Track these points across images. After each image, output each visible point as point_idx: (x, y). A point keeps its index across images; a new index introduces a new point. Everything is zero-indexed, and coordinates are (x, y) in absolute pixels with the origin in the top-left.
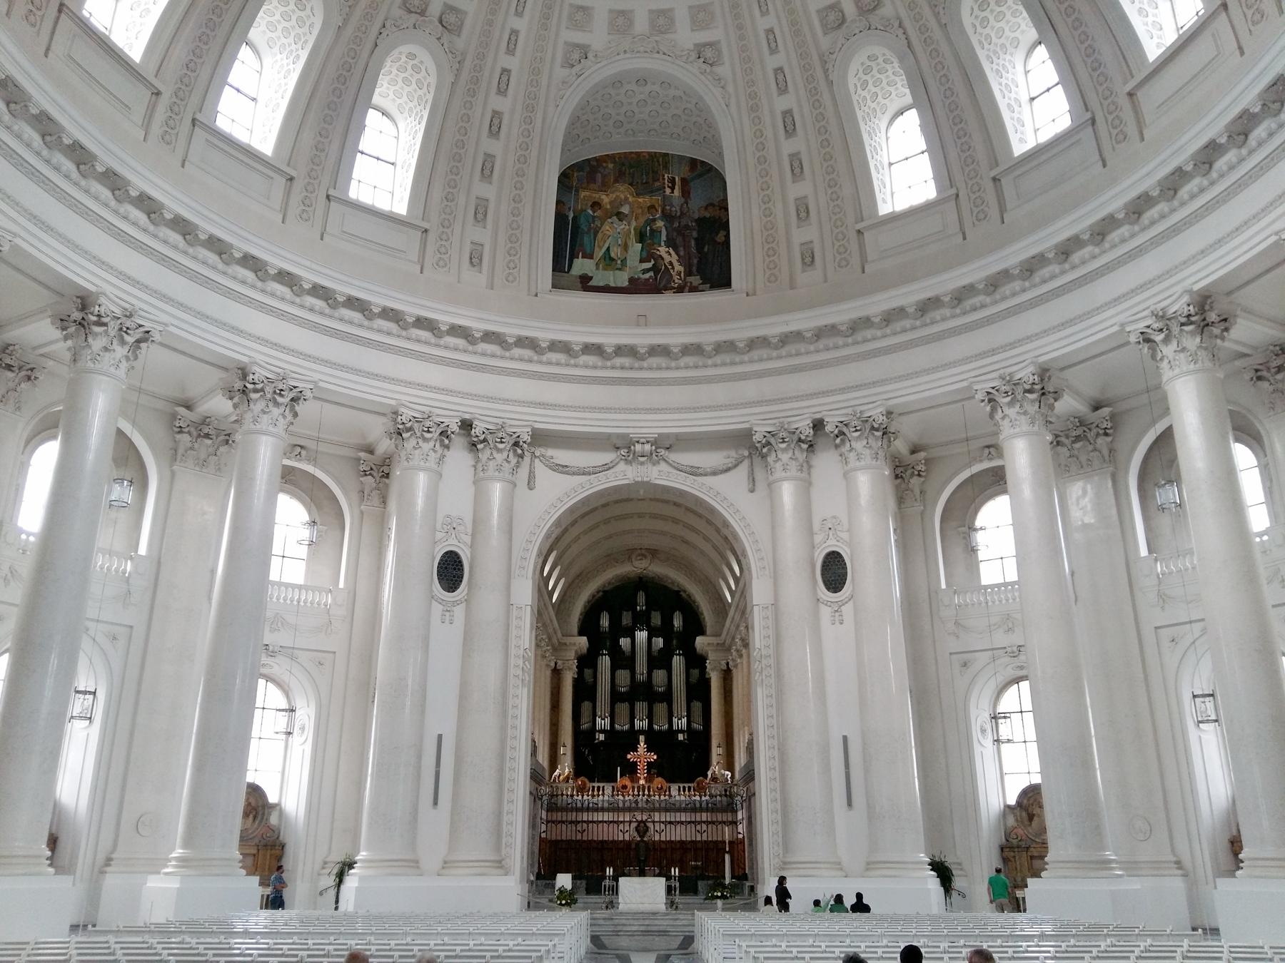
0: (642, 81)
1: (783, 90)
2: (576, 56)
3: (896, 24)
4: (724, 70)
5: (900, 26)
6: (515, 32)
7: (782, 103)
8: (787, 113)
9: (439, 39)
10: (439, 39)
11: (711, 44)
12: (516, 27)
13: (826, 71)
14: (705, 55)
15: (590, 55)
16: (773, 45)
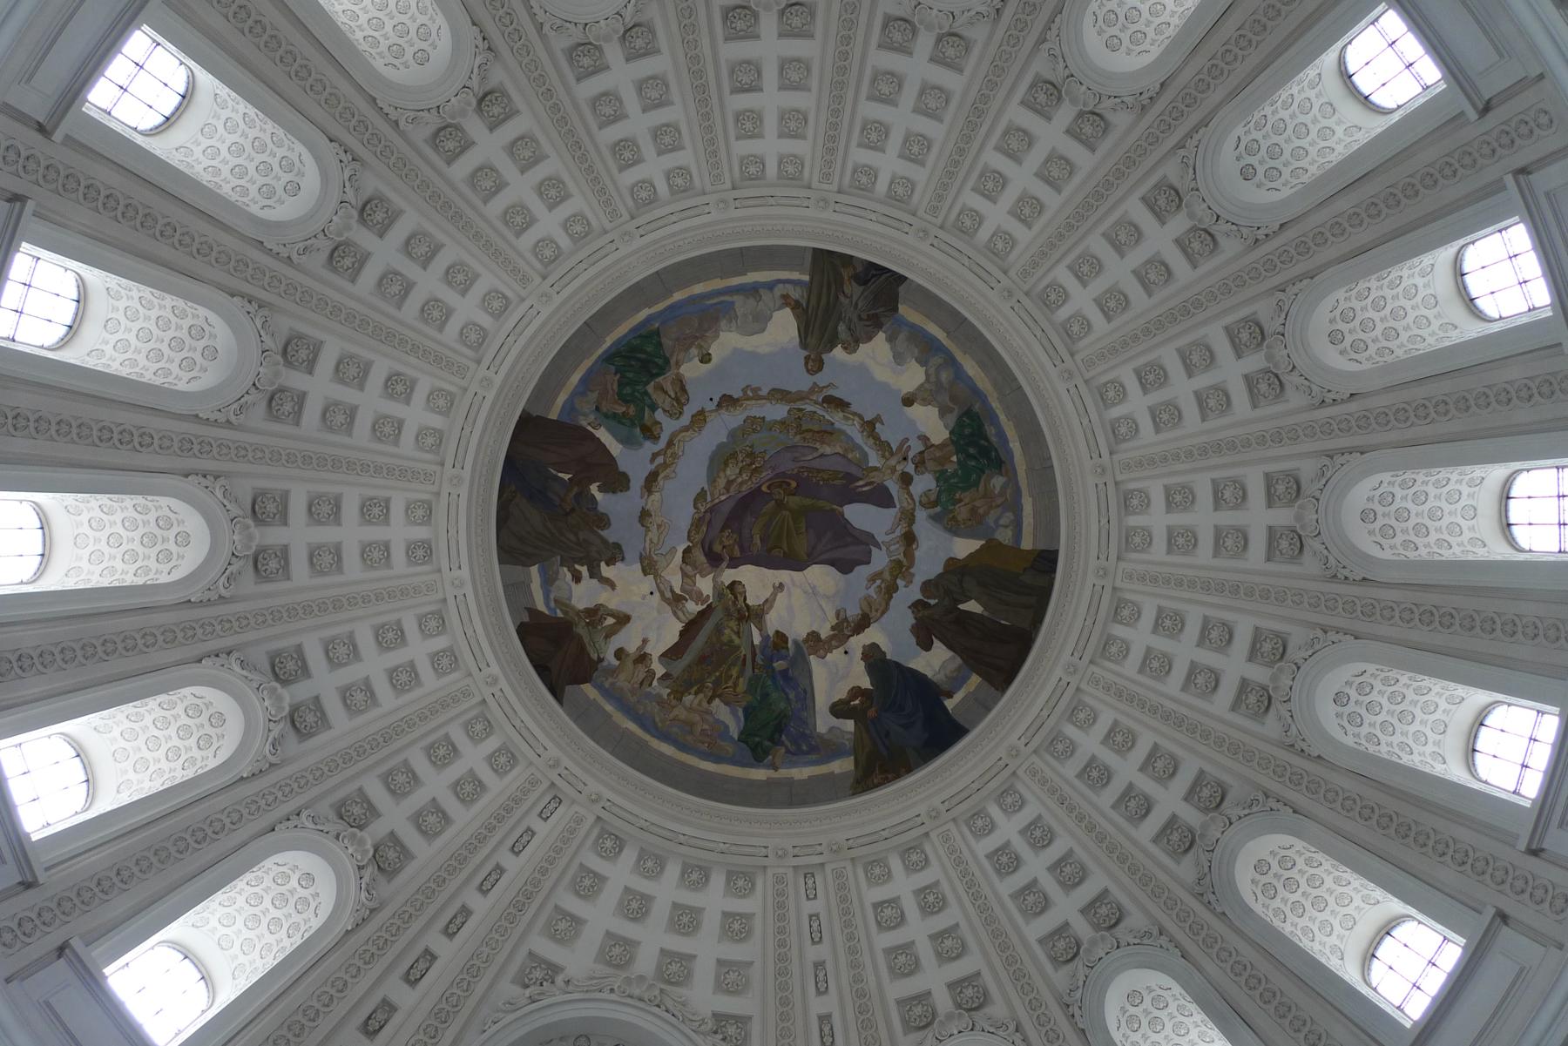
2: (538, 974)
6: (466, 912)
9: (360, 868)
10: (360, 868)
12: (471, 905)
15: (559, 979)
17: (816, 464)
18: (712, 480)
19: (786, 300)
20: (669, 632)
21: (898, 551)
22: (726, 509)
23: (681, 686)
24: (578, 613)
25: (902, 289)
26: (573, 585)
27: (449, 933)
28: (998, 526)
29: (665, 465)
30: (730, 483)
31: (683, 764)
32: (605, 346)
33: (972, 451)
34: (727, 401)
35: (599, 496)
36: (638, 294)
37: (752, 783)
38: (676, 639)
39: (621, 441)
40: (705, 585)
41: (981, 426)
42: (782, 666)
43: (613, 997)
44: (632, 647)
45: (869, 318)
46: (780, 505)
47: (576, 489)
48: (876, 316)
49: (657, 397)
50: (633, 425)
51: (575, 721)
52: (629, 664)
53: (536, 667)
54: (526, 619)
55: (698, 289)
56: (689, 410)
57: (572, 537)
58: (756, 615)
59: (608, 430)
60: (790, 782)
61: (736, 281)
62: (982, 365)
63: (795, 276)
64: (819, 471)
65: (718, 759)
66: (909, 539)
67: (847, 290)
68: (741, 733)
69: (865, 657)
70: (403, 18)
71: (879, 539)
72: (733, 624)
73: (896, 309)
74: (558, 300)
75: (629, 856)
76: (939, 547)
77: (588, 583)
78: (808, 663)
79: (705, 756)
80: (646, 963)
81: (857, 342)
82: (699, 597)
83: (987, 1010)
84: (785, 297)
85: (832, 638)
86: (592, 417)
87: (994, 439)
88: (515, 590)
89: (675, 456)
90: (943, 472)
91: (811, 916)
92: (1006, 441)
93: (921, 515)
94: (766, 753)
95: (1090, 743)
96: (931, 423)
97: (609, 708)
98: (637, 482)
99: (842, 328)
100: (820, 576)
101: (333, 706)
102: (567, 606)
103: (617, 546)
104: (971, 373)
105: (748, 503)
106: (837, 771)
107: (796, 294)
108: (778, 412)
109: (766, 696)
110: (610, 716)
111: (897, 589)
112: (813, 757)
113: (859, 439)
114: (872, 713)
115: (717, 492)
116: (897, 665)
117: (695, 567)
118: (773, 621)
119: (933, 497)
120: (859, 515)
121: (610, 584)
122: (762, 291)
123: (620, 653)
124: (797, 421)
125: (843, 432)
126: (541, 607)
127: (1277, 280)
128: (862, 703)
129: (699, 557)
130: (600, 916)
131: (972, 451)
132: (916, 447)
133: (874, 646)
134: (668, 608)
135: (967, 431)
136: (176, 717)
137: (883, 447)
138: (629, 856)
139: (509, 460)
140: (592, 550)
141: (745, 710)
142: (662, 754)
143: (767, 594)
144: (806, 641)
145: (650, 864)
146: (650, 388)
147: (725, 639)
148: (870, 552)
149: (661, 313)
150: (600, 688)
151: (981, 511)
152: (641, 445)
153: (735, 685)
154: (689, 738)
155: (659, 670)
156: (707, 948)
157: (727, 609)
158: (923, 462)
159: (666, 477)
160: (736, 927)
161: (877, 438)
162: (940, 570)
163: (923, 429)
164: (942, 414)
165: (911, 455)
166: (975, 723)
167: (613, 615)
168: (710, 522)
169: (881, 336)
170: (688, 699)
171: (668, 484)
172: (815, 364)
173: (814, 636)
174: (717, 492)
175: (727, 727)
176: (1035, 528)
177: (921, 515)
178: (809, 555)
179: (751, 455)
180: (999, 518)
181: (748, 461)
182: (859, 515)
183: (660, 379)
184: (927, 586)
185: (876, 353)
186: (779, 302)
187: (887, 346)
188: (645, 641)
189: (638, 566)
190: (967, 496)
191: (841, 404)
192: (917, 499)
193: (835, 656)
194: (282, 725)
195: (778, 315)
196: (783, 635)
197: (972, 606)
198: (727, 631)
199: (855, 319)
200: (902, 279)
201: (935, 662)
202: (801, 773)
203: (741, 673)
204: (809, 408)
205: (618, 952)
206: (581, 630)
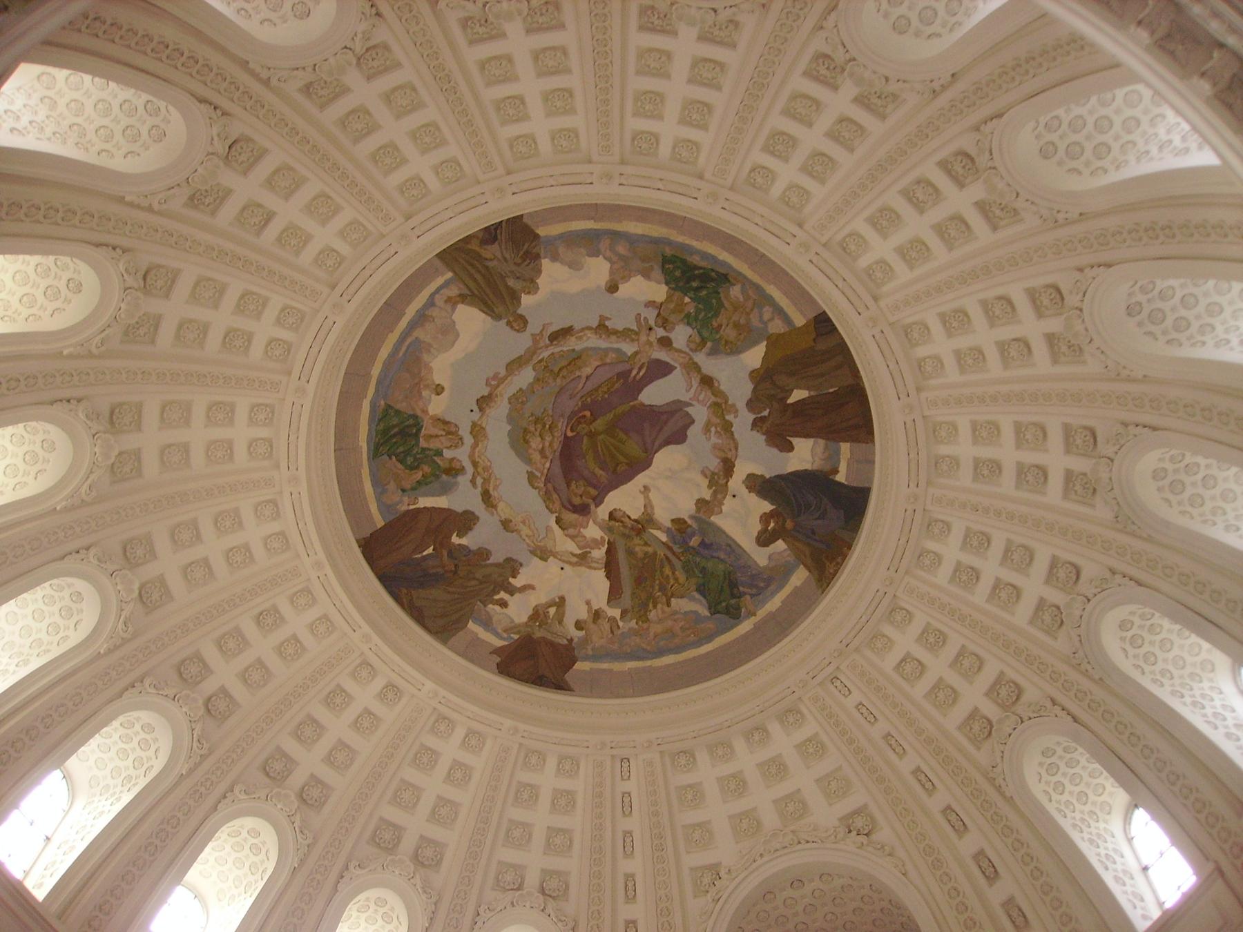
0: (796, 883)
1: (961, 828)
2: (706, 880)
3: (1048, 704)
4: (884, 834)
5: (1054, 702)
6: (630, 877)
7: (968, 845)
8: (979, 855)
11: (857, 812)
13: (998, 788)
14: (858, 826)
16: (928, 785)
17: (590, 386)
18: (529, 461)
19: (452, 302)
20: (599, 583)
21: (705, 395)
22: (557, 470)
23: (641, 610)
25: (525, 220)
26: (505, 610)
27: (631, 897)
28: (765, 323)
29: (486, 481)
30: (542, 452)
31: (685, 661)
33: (694, 284)
34: (484, 402)
35: (463, 541)
37: (745, 637)
38: (608, 583)
40: (593, 531)
41: (684, 262)
43: (765, 859)
44: (583, 614)
46: (592, 435)
47: (445, 553)
48: (527, 253)
49: (435, 444)
50: (437, 477)
52: (592, 626)
54: (498, 660)
55: (384, 353)
56: (465, 432)
57: (473, 583)
59: (426, 495)
60: (772, 616)
63: (440, 281)
64: (596, 390)
65: (710, 638)
66: (707, 381)
67: (489, 256)
69: (750, 489)
71: (685, 397)
72: (637, 541)
73: (537, 236)
74: (302, 473)
75: (703, 757)
76: (737, 372)
77: (514, 601)
78: (711, 525)
79: (698, 643)
80: (770, 819)
81: (532, 281)
82: (597, 543)
83: (1024, 699)
84: (448, 300)
85: (715, 493)
86: (406, 499)
87: (702, 264)
88: (471, 652)
89: (486, 469)
90: (688, 316)
91: (856, 707)
92: (714, 258)
93: (700, 358)
94: (738, 609)
95: (965, 449)
96: (646, 289)
97: (605, 666)
98: (477, 506)
99: (511, 282)
100: (666, 458)
101: (436, 832)
103: (509, 560)
105: (568, 453)
106: (798, 584)
107: (453, 291)
108: (526, 377)
109: (703, 571)
110: (611, 671)
112: (772, 587)
113: (603, 344)
114: (789, 524)
115: (539, 465)
116: (779, 477)
117: (575, 526)
118: (663, 515)
119: (698, 339)
120: (655, 394)
121: (528, 587)
122: (428, 313)
123: (579, 625)
124: (547, 370)
125: (587, 349)
126: (500, 643)
128: (776, 523)
129: (570, 517)
130: (717, 811)
131: (694, 284)
132: (651, 315)
133: (751, 477)
134: (583, 569)
135: (678, 273)
137: (626, 334)
138: (703, 757)
139: (384, 579)
140: (498, 578)
142: (668, 666)
143: (641, 501)
144: (698, 510)
146: (423, 443)
147: (640, 555)
148: (687, 414)
149: (377, 390)
150: (587, 658)
151: (742, 321)
152: (456, 484)
153: (676, 580)
155: (615, 613)
156: (803, 779)
157: (624, 535)
160: (812, 749)
161: (615, 332)
164: (646, 275)
166: (871, 480)
168: (555, 489)
169: (546, 263)
170: (652, 615)
171: (500, 493)
172: (519, 323)
173: (701, 503)
174: (539, 465)
175: (696, 612)
176: (795, 305)
177: (700, 358)
180: (761, 317)
181: (539, 426)
182: (655, 394)
184: (750, 405)
185: (554, 276)
186: (449, 307)
187: (557, 265)
188: (588, 603)
189: (536, 560)
190: (722, 319)
191: (566, 332)
194: (418, 876)
197: (798, 395)
198: (637, 549)
199: (514, 268)
201: (804, 454)
202: (775, 603)
203: (673, 571)
204: (545, 354)
205: (746, 824)
206: (538, 634)
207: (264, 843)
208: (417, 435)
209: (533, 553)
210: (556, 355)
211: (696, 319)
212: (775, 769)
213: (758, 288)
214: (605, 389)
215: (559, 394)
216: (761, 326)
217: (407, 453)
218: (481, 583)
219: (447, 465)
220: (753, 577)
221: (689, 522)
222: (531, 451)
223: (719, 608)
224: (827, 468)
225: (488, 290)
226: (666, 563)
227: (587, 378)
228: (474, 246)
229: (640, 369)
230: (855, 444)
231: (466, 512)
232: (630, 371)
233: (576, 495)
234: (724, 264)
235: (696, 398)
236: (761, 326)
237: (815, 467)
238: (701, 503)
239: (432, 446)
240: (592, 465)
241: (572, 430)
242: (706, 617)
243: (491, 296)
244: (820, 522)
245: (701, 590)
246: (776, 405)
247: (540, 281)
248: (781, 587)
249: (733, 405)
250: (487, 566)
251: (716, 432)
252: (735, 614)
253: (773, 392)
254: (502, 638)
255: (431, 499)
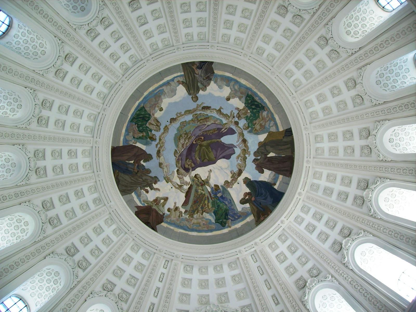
9: (116, 303)
17: (207, 129)
18: (177, 146)
19: (179, 83)
20: (182, 197)
21: (242, 146)
22: (185, 153)
23: (192, 213)
24: (151, 202)
26: (147, 194)
28: (270, 127)
29: (161, 147)
30: (183, 145)
32: (129, 117)
33: (253, 107)
34: (173, 120)
35: (144, 164)
36: (133, 98)
37: (224, 234)
38: (185, 199)
39: (145, 145)
40: (187, 179)
41: (253, 98)
42: (220, 195)
44: (172, 207)
45: (207, 78)
46: (201, 146)
47: (137, 165)
49: (151, 127)
50: (147, 138)
51: (163, 235)
52: (173, 211)
53: (145, 223)
54: (137, 210)
55: (151, 89)
56: (162, 127)
57: (141, 180)
58: (206, 182)
60: (236, 229)
61: (161, 83)
62: (247, 80)
63: (179, 74)
64: (209, 131)
65: (211, 231)
66: (244, 141)
67: (197, 72)
68: (216, 220)
69: (245, 182)
70: (34, 43)
71: (235, 144)
72: (200, 188)
73: (214, 73)
76: (255, 141)
81: (206, 87)
82: (187, 183)
84: (178, 81)
85: (232, 180)
86: (133, 141)
87: (259, 101)
88: (130, 202)
93: (245, 132)
94: (225, 223)
96: (238, 103)
97: (172, 228)
98: (154, 155)
99: (199, 84)
100: (221, 163)
102: (147, 201)
103: (156, 177)
104: (244, 83)
105: (191, 149)
106: (249, 221)
107: (181, 79)
108: (189, 117)
109: (218, 206)
111: (246, 158)
112: (240, 219)
113: (217, 116)
118: (212, 182)
119: (247, 126)
120: (226, 140)
121: (158, 189)
122: (170, 82)
123: (169, 210)
124: (197, 118)
125: (212, 116)
126: (140, 204)
127: (325, 22)
128: (249, 197)
129: (182, 171)
131: (253, 107)
132: (236, 112)
134: (179, 190)
135: (250, 101)
136: (45, 277)
137: (226, 116)
139: (113, 164)
141: (214, 213)
142: (194, 236)
143: (207, 174)
144: (225, 184)
145: (203, 270)
146: (148, 125)
147: (199, 193)
150: (167, 223)
151: (263, 124)
152: (151, 143)
153: (208, 206)
154: (200, 228)
155: (183, 210)
158: (240, 116)
159: (163, 150)
161: (223, 114)
162: (257, 147)
163: (236, 106)
164: (240, 99)
165: (235, 115)
166: (286, 190)
167: (162, 199)
168: (181, 159)
169: (212, 82)
170: (195, 216)
171: (165, 153)
172: (195, 99)
173: (227, 182)
175: (210, 220)
176: (282, 123)
177: (245, 132)
178: (215, 158)
179: (186, 134)
180: (270, 124)
181: (186, 136)
182: (226, 140)
183: (149, 121)
184: (255, 154)
185: (212, 88)
186: (177, 84)
187: (215, 85)
188: (175, 203)
189: (164, 181)
190: (257, 121)
191: (208, 108)
192: (242, 128)
193: (235, 185)
195: (177, 88)
196: (217, 185)
197: (272, 154)
198: (199, 191)
199: (202, 80)
200: (212, 63)
201: (266, 176)
202: (238, 225)
203: (208, 202)
204: (199, 113)
206: (154, 207)
207: (27, 229)
208: (147, 121)
209: (165, 178)
210: (201, 114)
211: (249, 119)
212: (220, 283)
213: (272, 114)
214: (212, 132)
215: (196, 128)
216: (268, 127)
217: (141, 125)
218: (143, 181)
219: (151, 136)
220: (235, 214)
221: (220, 187)
222: (179, 143)
223: (219, 221)
224: (273, 182)
225: (191, 84)
226: (207, 199)
227: (208, 126)
228: (194, 67)
229: (225, 129)
230: (285, 177)
231: (150, 155)
232: (222, 129)
233: (187, 164)
234: (265, 103)
235: (238, 145)
236: (268, 127)
237: (268, 181)
238: (227, 182)
239: (150, 127)
240: (196, 156)
241: (195, 142)
242: (213, 223)
243: (191, 86)
244: (264, 201)
245: (215, 213)
246: (263, 156)
247: (208, 88)
248: (243, 220)
249: (250, 152)
250: (148, 176)
251: (241, 159)
252: (224, 225)
253: (263, 151)
254: (141, 203)
255: (141, 145)
